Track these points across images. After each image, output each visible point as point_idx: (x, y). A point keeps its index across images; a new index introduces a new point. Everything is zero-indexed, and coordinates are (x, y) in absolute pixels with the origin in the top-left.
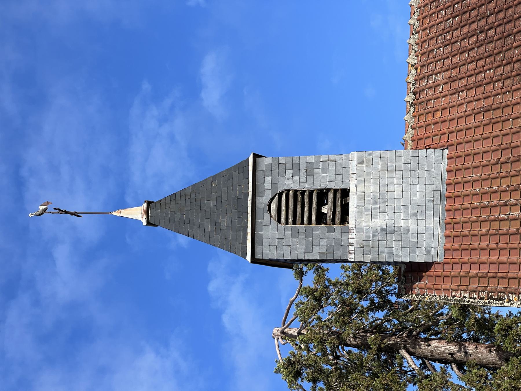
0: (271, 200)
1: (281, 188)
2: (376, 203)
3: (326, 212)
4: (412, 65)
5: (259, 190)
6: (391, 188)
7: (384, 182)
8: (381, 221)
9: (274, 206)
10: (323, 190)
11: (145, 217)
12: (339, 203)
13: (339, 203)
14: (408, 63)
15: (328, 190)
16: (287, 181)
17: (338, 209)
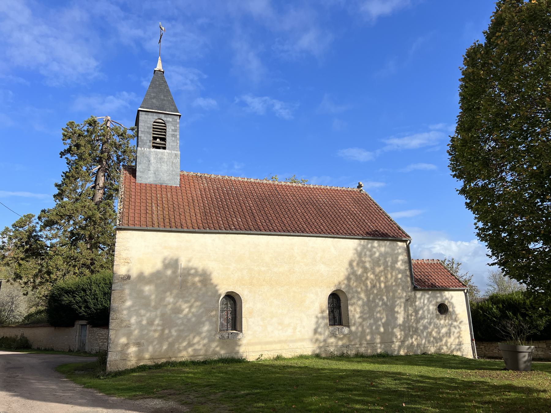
0: (163, 120)
1: (167, 124)
2: (160, 159)
6: (166, 165)
7: (168, 163)
9: (160, 121)
11: (158, 70)
12: (160, 145)
13: (160, 145)
15: (166, 142)
17: (158, 145)
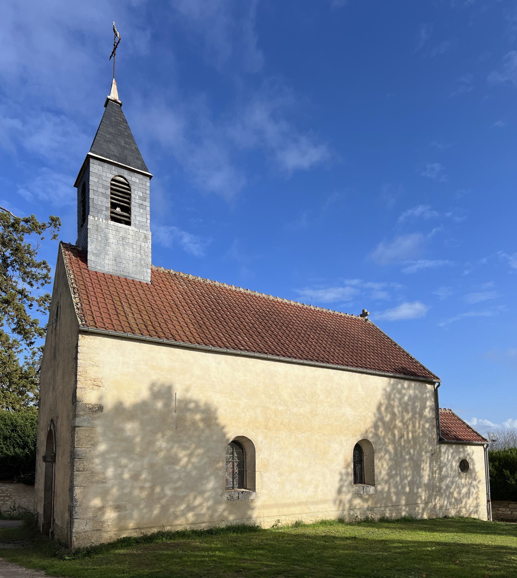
0: (125, 179)
1: (132, 187)
2: (123, 239)
3: (117, 210)
4: (188, 277)
5: (132, 174)
6: (131, 250)
7: (135, 247)
8: (112, 240)
9: (122, 179)
10: (131, 211)
11: (113, 99)
12: (122, 218)
13: (122, 218)
14: (189, 275)
15: (130, 214)
16: (136, 192)
17: (119, 217)
